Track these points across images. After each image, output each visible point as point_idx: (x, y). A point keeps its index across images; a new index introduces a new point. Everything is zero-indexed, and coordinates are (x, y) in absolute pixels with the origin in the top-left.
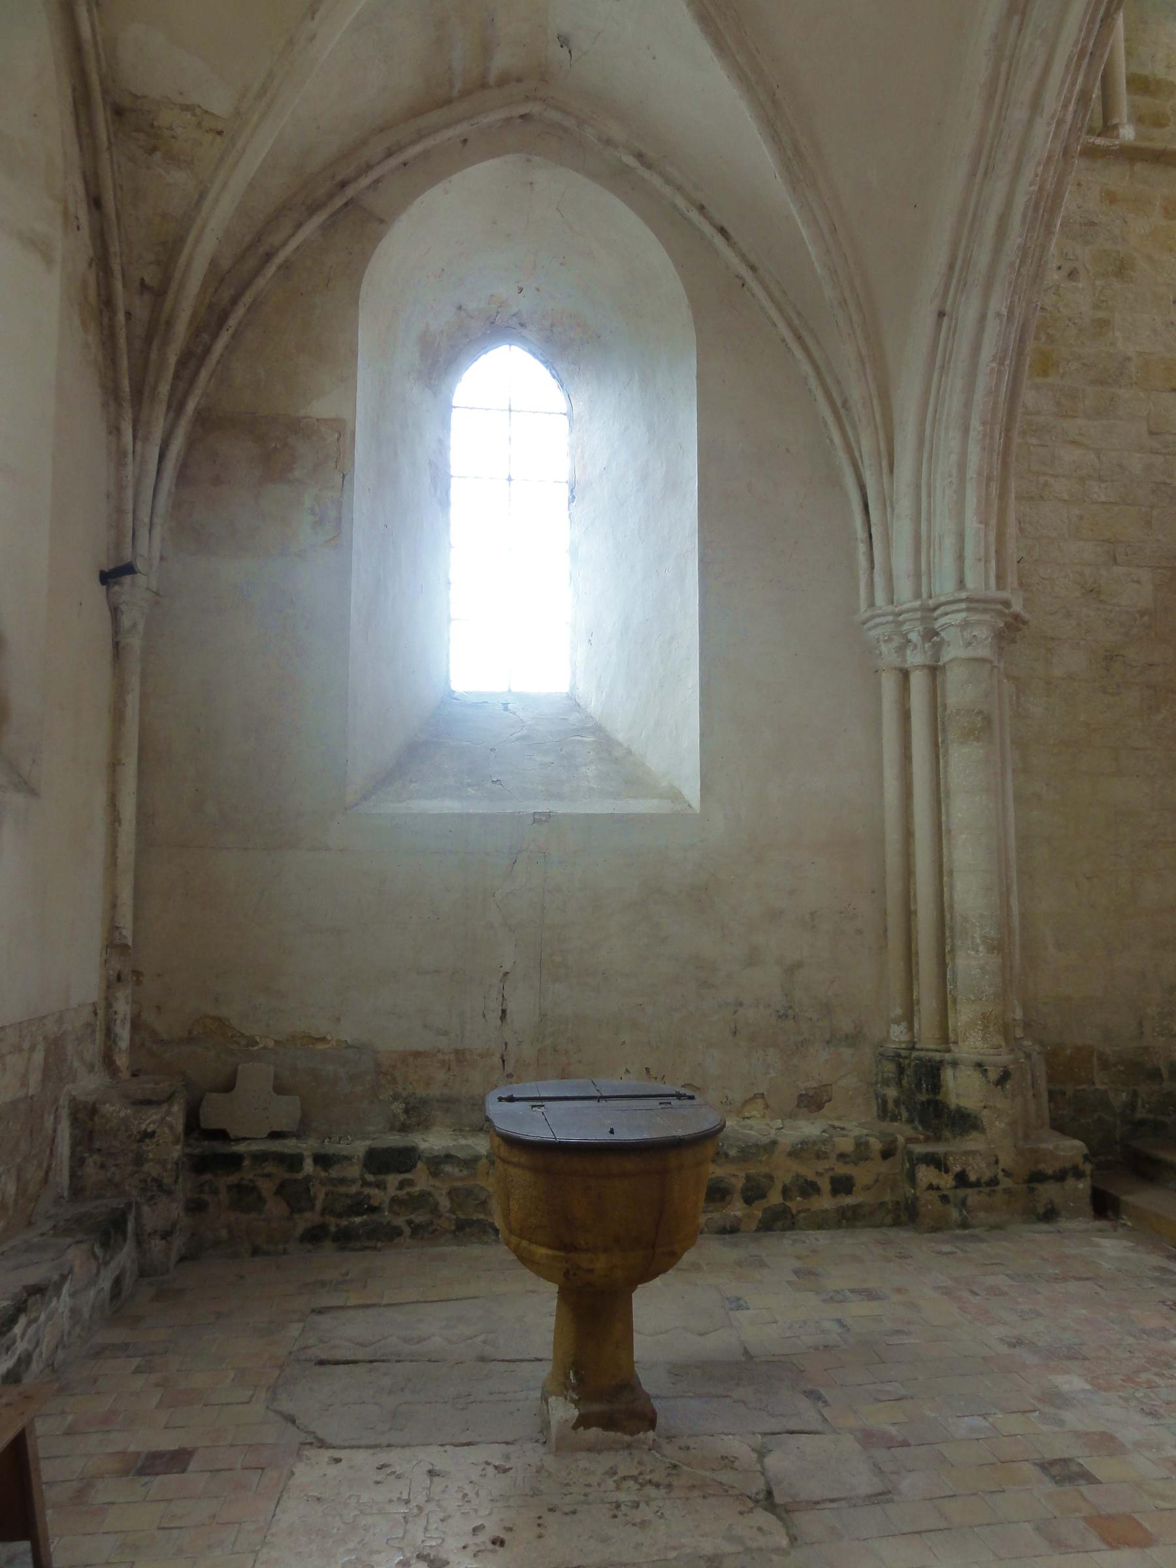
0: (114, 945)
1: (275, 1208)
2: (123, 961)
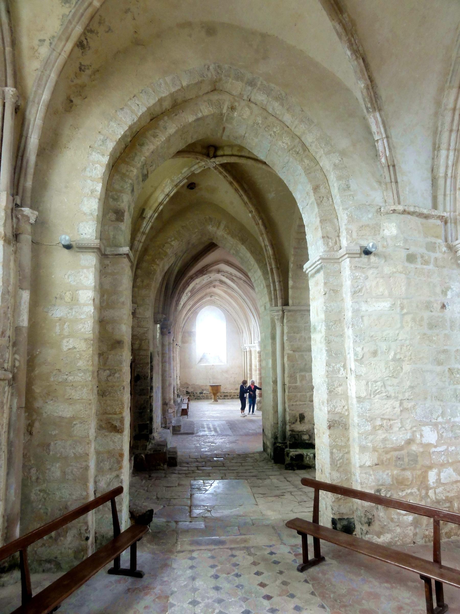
1: (193, 397)
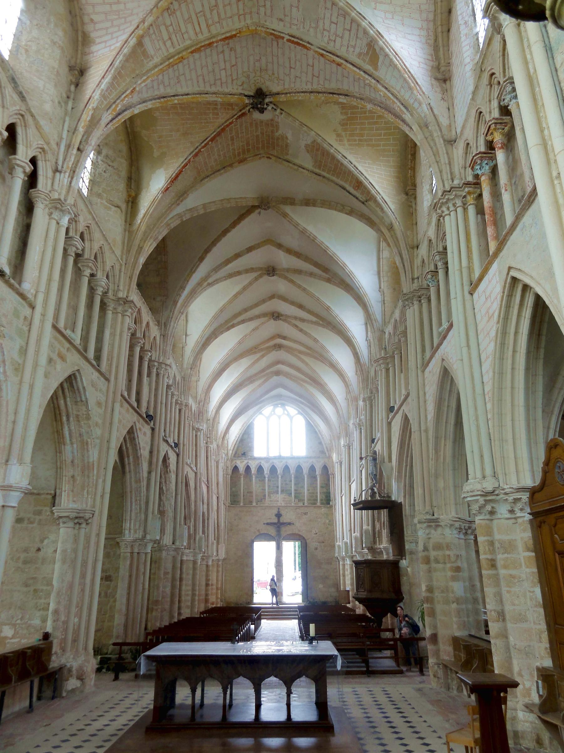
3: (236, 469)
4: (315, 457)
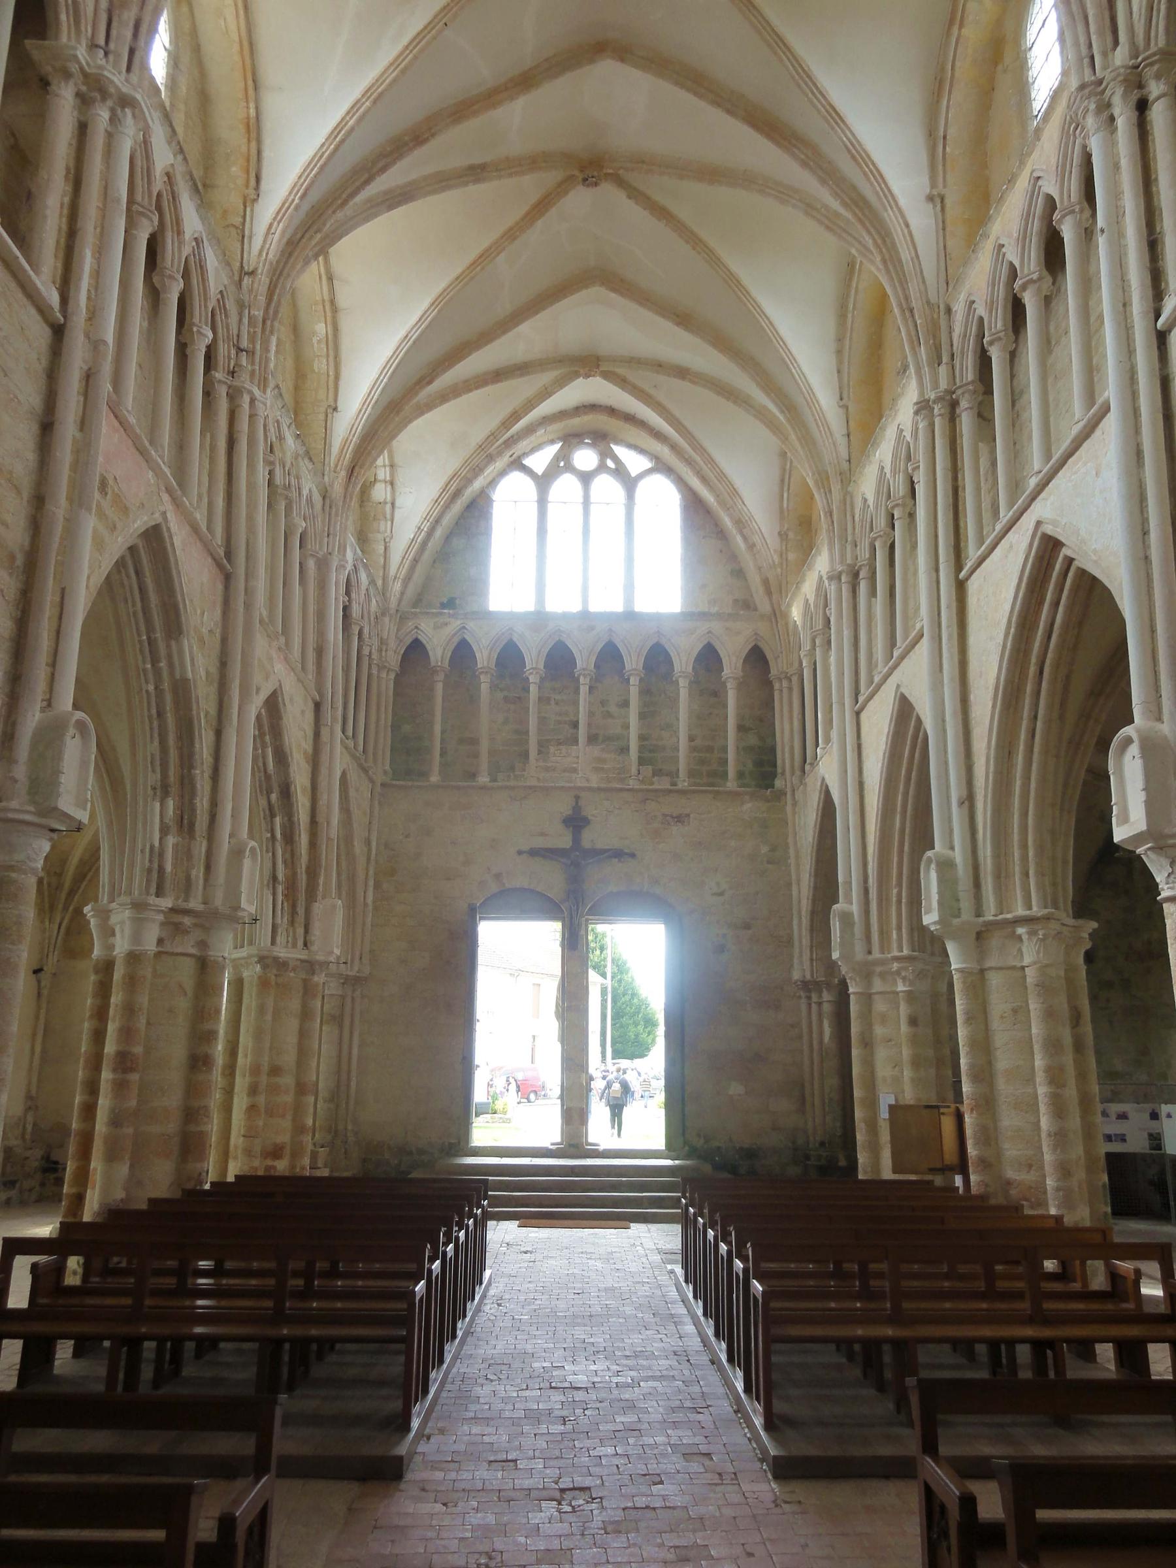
0: (29, 1097)
2: (32, 1102)
3: (415, 651)
4: (719, 616)
